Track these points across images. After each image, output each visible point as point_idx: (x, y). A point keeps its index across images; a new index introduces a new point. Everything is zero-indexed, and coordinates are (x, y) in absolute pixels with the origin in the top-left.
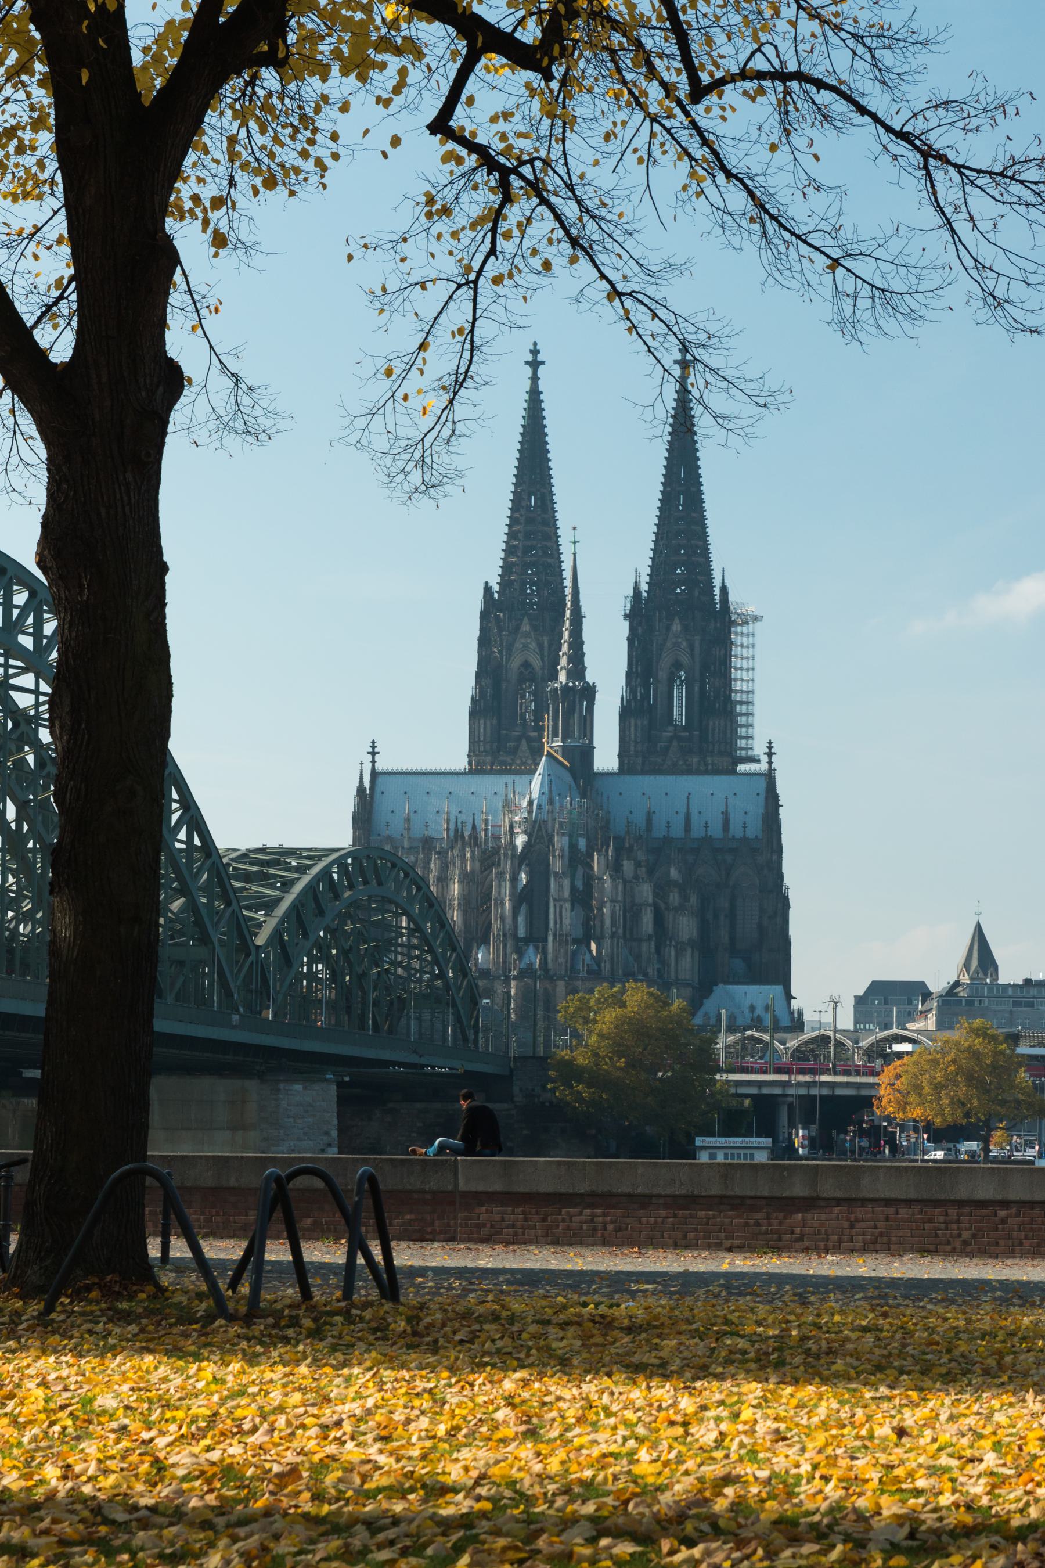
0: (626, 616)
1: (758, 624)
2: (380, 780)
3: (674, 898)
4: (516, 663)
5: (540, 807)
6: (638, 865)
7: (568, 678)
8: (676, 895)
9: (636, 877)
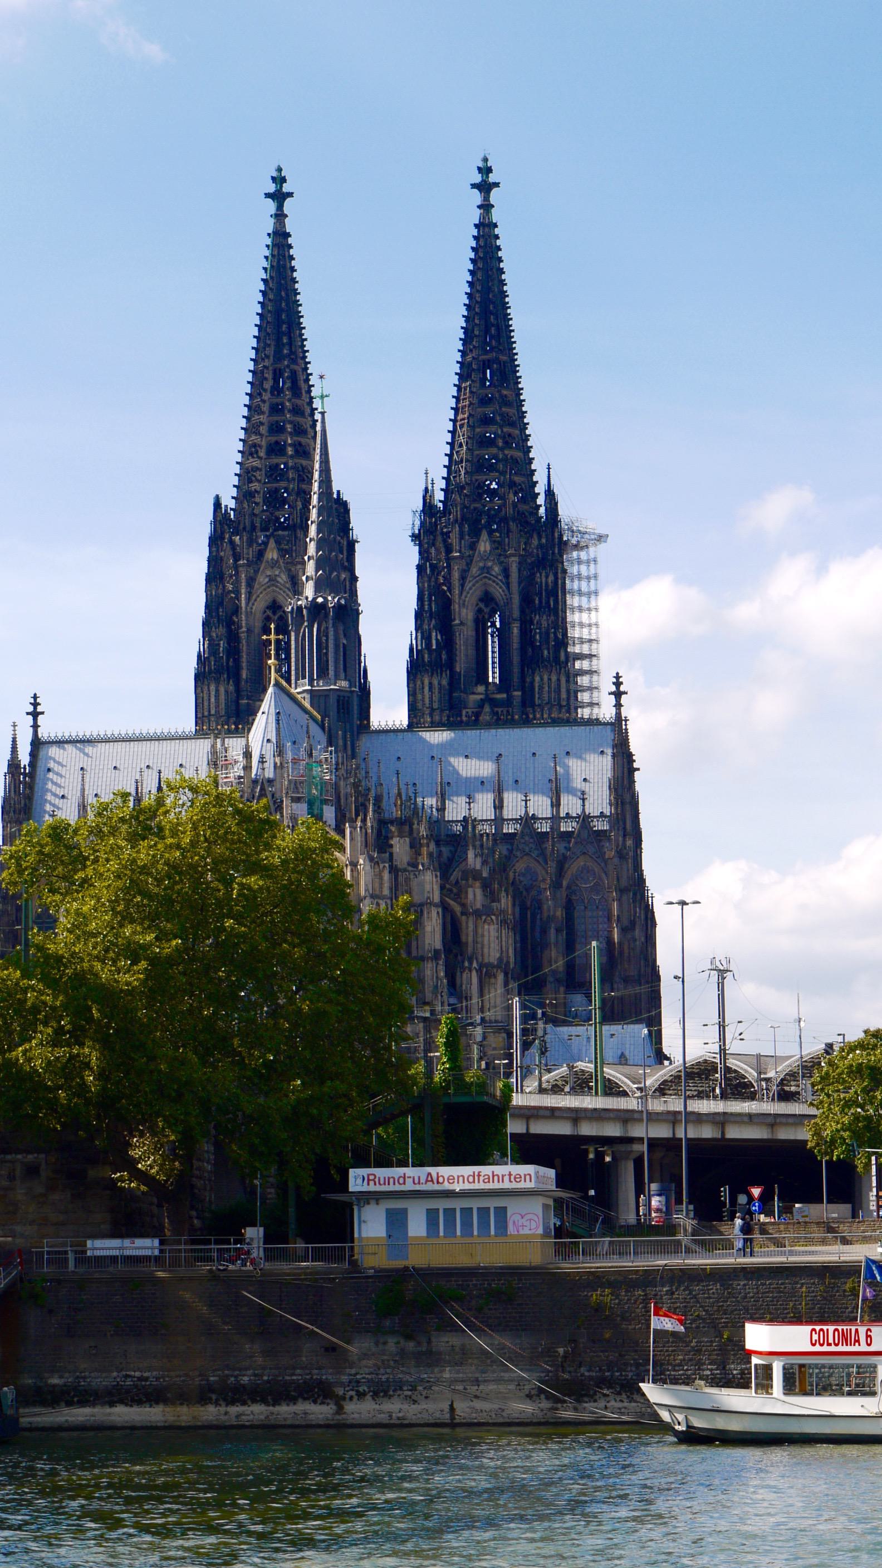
0: (415, 537)
1: (602, 546)
3: (475, 896)
5: (262, 760)
7: (318, 589)
8: (479, 892)
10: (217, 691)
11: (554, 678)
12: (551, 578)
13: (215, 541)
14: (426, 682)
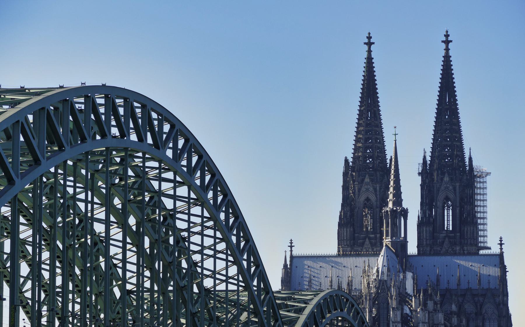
0: (419, 174)
1: (488, 177)
2: (295, 260)
4: (362, 198)
5: (382, 272)
6: (435, 303)
8: (456, 319)
9: (435, 310)
10: (347, 231)
11: (472, 228)
12: (471, 191)
13: (345, 174)
14: (425, 229)
